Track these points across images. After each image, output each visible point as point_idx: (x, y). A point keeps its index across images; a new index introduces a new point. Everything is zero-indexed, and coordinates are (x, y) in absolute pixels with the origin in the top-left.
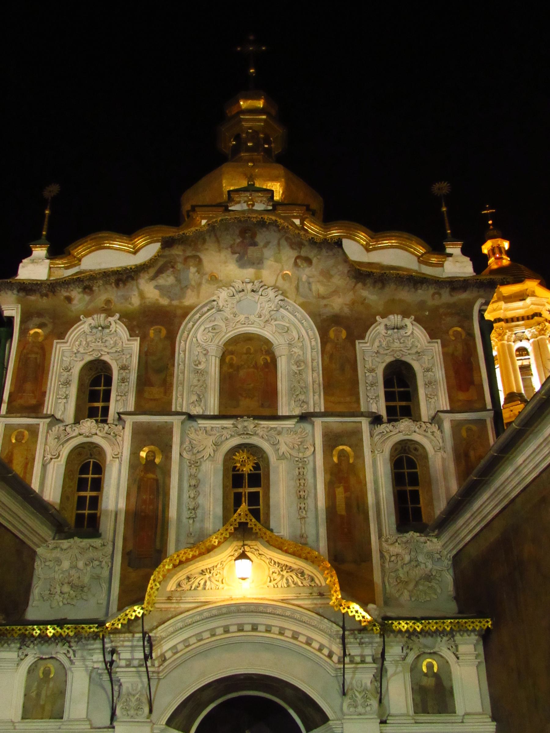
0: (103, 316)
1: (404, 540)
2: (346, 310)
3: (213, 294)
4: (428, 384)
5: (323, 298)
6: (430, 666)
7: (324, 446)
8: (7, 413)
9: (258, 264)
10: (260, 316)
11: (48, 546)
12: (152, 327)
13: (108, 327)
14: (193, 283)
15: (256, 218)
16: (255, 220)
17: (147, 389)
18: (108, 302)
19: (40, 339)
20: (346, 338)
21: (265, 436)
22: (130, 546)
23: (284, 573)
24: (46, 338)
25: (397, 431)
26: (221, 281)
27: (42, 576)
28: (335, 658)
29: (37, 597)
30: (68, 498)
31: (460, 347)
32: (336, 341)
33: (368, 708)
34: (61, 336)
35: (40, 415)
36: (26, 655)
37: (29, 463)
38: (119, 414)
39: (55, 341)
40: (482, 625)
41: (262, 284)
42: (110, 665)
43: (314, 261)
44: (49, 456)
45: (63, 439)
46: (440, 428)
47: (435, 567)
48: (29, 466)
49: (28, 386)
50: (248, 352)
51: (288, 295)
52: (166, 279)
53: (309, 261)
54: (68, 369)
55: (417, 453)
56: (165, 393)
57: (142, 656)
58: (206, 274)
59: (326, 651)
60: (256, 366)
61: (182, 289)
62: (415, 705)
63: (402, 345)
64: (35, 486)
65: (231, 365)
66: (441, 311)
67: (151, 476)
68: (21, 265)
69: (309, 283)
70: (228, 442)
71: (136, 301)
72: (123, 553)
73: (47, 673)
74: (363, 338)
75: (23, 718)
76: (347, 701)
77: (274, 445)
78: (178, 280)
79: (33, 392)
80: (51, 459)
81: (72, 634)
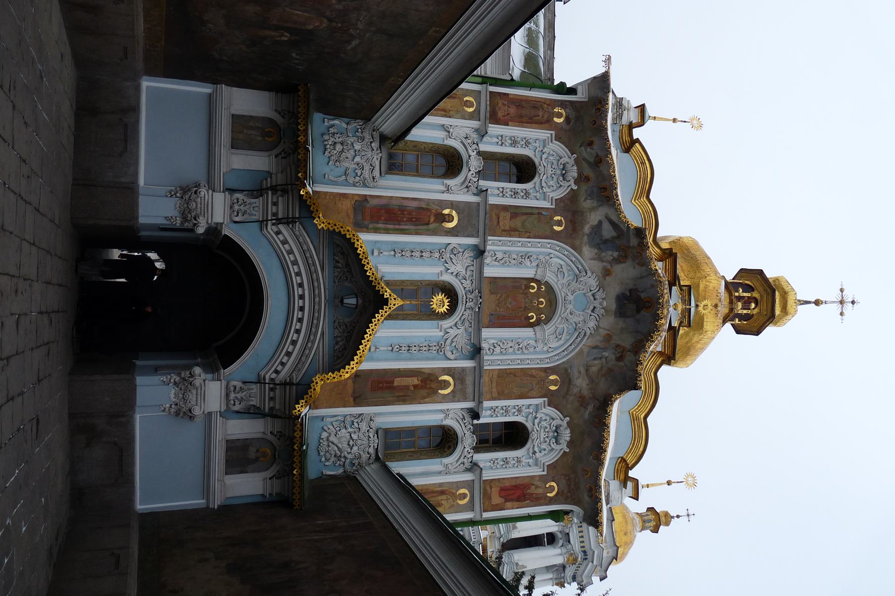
0: (576, 175)
1: (371, 436)
3: (593, 273)
4: (506, 461)
5: (587, 370)
7: (455, 368)
8: (491, 92)
10: (571, 314)
14: (603, 254)
17: (508, 215)
18: (587, 179)
19: (556, 119)
22: (373, 202)
23: (345, 334)
27: (350, 127)
28: (274, 376)
31: (540, 491)
34: (558, 138)
37: (446, 114)
42: (274, 189)
43: (621, 364)
44: (451, 130)
45: (466, 142)
46: (468, 470)
49: (512, 110)
52: (608, 232)
53: (620, 358)
54: (527, 143)
55: (446, 449)
57: (280, 216)
59: (280, 368)
60: (527, 309)
61: (598, 244)
62: (233, 441)
63: (542, 439)
64: (428, 119)
65: (529, 287)
66: (573, 476)
67: (432, 220)
69: (601, 358)
71: (587, 204)
72: (366, 195)
74: (549, 405)
76: (239, 384)
77: (456, 325)
78: (606, 241)
81: (300, 157)
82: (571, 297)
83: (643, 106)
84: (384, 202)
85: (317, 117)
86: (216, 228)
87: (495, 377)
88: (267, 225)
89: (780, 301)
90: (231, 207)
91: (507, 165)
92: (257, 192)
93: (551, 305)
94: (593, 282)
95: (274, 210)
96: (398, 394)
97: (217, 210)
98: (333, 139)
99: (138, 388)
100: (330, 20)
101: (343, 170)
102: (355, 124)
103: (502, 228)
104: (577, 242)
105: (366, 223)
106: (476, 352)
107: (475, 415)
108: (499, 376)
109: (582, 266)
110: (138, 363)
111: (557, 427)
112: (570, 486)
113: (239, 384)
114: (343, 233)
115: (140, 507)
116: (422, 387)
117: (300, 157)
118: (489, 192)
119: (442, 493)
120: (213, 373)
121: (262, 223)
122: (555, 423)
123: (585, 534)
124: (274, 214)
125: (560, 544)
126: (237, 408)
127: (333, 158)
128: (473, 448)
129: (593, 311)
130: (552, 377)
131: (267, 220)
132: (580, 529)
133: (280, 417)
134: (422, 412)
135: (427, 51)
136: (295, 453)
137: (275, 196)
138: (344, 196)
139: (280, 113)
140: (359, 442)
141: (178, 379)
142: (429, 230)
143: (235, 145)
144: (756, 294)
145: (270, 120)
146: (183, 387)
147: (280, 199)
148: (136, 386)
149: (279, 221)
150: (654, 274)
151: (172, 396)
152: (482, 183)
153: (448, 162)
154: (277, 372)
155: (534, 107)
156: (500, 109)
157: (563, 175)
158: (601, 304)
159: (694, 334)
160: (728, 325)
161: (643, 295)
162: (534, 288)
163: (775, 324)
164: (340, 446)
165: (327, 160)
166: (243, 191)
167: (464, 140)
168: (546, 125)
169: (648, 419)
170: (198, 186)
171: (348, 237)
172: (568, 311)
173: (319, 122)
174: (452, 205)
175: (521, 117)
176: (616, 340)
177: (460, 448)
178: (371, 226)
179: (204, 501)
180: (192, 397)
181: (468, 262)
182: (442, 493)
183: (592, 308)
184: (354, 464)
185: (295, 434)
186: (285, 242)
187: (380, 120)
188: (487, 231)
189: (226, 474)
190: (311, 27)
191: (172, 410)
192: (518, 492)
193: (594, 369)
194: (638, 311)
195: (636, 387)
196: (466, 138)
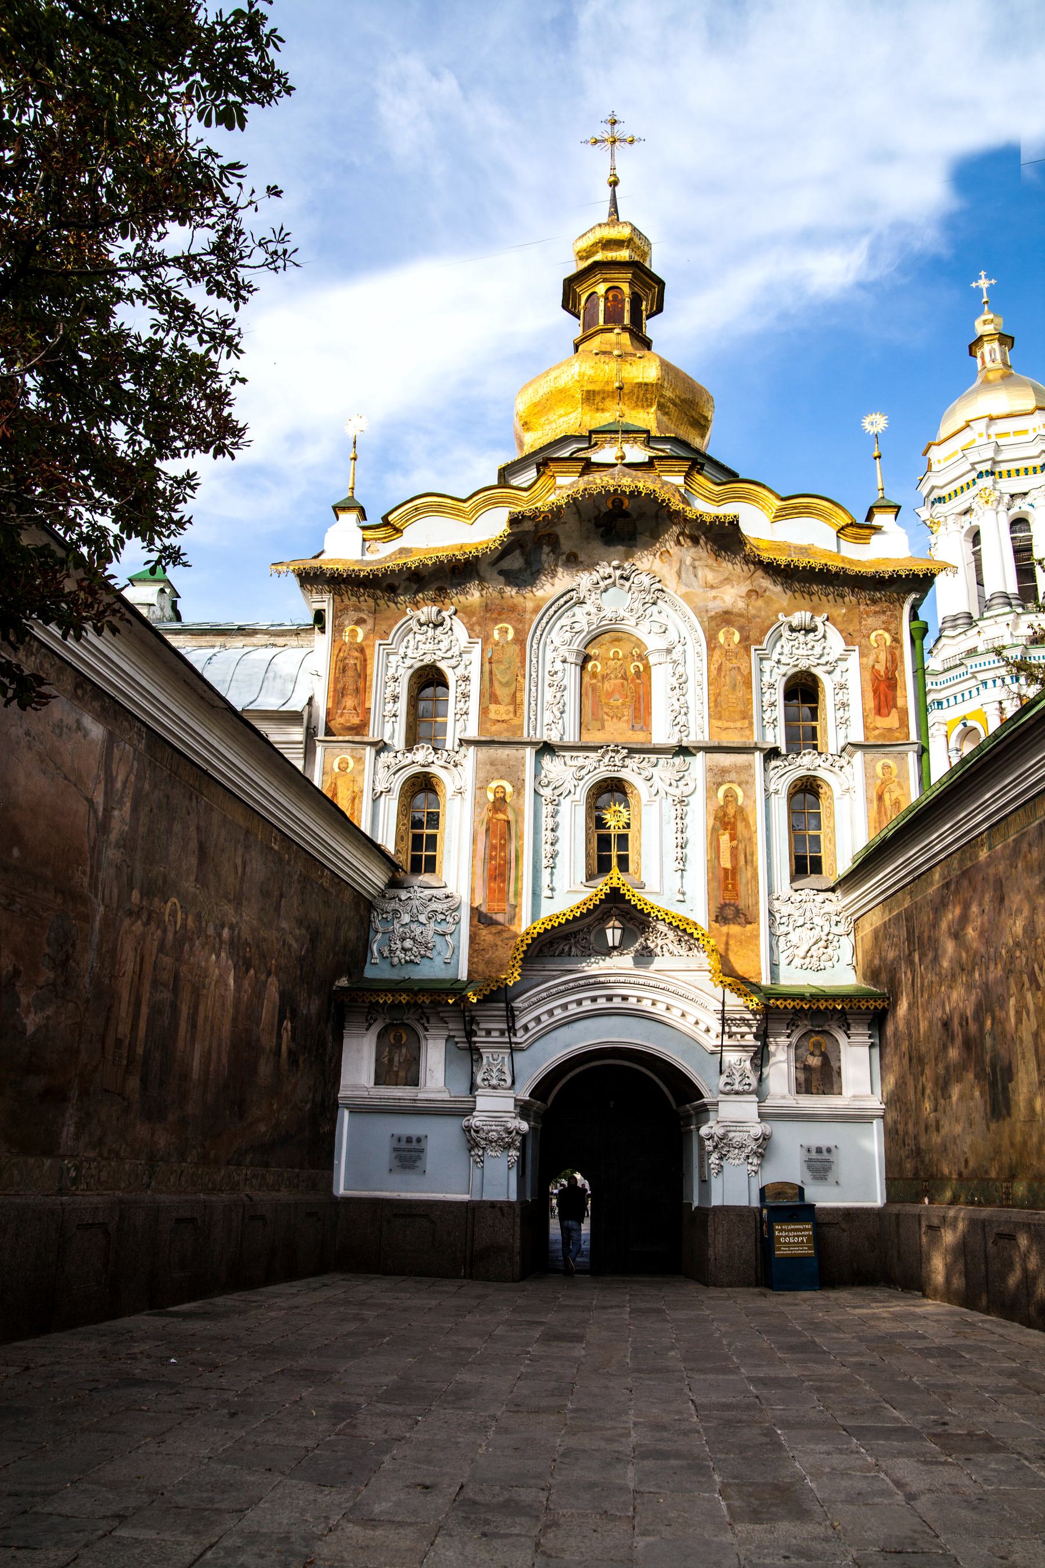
0: (435, 609)
2: (741, 604)
5: (712, 587)
6: (818, 1045)
9: (630, 540)
11: (384, 896)
12: (496, 624)
13: (441, 624)
14: (546, 566)
15: (629, 486)
16: (628, 490)
17: (493, 707)
19: (359, 639)
20: (739, 642)
21: (635, 769)
24: (366, 638)
25: (798, 764)
26: (582, 562)
27: (381, 929)
28: (713, 1034)
29: (376, 954)
30: (402, 838)
31: (883, 657)
32: (727, 647)
33: (747, 1087)
35: (366, 739)
36: (375, 1020)
38: (460, 740)
39: (378, 642)
40: (877, 1004)
41: (634, 568)
42: (470, 1034)
47: (835, 930)
48: (357, 801)
49: (349, 702)
50: (616, 657)
51: (667, 583)
52: (515, 562)
53: (695, 541)
56: (515, 712)
58: (563, 554)
60: (624, 677)
61: (532, 574)
65: (594, 675)
68: (327, 536)
69: (695, 568)
70: (591, 775)
73: (398, 1039)
74: (761, 643)
75: (375, 1084)
76: (724, 1079)
78: (528, 563)
79: (355, 709)
80: (382, 792)
82: (608, 613)
83: (335, 508)
84: (479, 884)
85: (369, 972)
86: (521, 1107)
87: (719, 724)
88: (516, 1043)
89: (611, 250)
90: (494, 1088)
91: (422, 705)
92: (474, 1053)
93: (618, 640)
94: (585, 580)
95: (497, 1034)
96: (742, 862)
97: (497, 1107)
98: (398, 952)
99: (729, 1202)
100: (269, 974)
101: (437, 939)
102: (378, 924)
103: (511, 715)
104: (530, 605)
105: (507, 909)
106: (683, 751)
107: (772, 753)
108: (720, 718)
109: (562, 596)
110: (696, 1203)
111: (792, 630)
112: (876, 612)
113: (724, 1079)
114: (525, 948)
115: (878, 1200)
116: (734, 828)
117: (427, 1002)
118: (462, 737)
119: (880, 798)
120: (707, 1111)
121: (514, 1049)
122: (786, 633)
123: (1012, 466)
124: (502, 1033)
125: (1029, 509)
126: (753, 1080)
127: (422, 952)
128: (820, 754)
129: (627, 579)
130: (721, 637)
131: (510, 1043)
132: (1005, 474)
133: (766, 1028)
134: (768, 828)
135: (295, 847)
136: (814, 1007)
137: (480, 1033)
138: (473, 938)
139: (370, 1025)
140: (808, 914)
141: (715, 1155)
142: (517, 821)
143: (414, 1081)
144: (601, 289)
145: (380, 1036)
146: (727, 1149)
147: (482, 1026)
148: (723, 1206)
149: (512, 1030)
150: (575, 499)
151: (737, 1162)
152: (449, 746)
153: (421, 791)
154: (708, 1030)
155: (344, 670)
156: (349, 721)
157: (436, 626)
158: (616, 568)
159: (662, 396)
160: (652, 328)
161: (604, 510)
162: (595, 666)
163: (645, 254)
164: (813, 941)
165: (425, 960)
166: (472, 1072)
167: (392, 770)
168: (368, 652)
169: (783, 496)
170: (468, 1129)
171: (530, 941)
172: (627, 615)
173: (375, 970)
174: (481, 788)
175: (357, 690)
176: (671, 545)
177: (820, 773)
178: (512, 901)
179: (875, 1122)
180: (737, 1137)
181: (558, 761)
182: (880, 798)
183: (622, 581)
184: (837, 923)
185: (790, 1007)
186: (538, 1020)
187: (371, 890)
188: (516, 739)
189: (841, 1094)
190: (277, 996)
191: (756, 1161)
192: (883, 690)
193: (710, 576)
194: (626, 514)
195: (734, 524)
196: (388, 767)
